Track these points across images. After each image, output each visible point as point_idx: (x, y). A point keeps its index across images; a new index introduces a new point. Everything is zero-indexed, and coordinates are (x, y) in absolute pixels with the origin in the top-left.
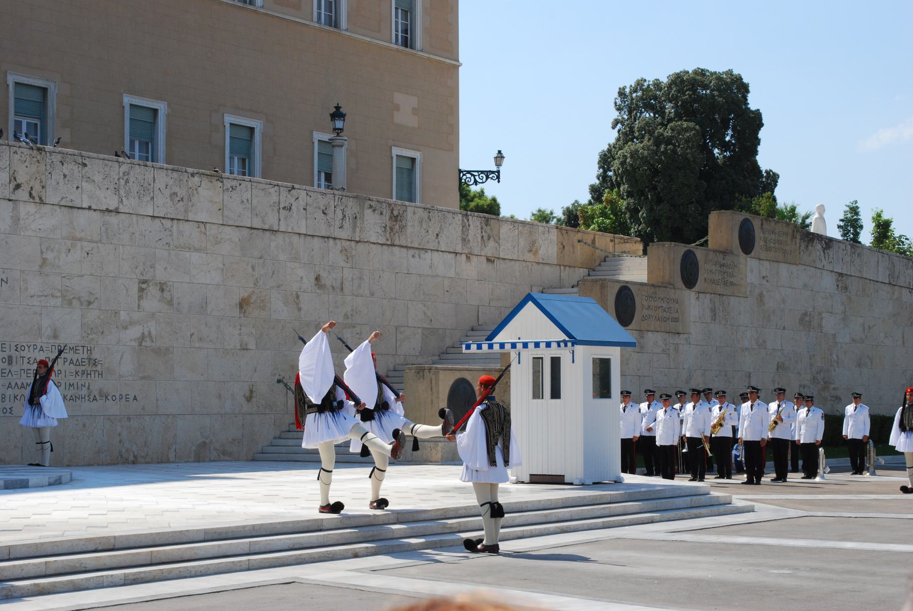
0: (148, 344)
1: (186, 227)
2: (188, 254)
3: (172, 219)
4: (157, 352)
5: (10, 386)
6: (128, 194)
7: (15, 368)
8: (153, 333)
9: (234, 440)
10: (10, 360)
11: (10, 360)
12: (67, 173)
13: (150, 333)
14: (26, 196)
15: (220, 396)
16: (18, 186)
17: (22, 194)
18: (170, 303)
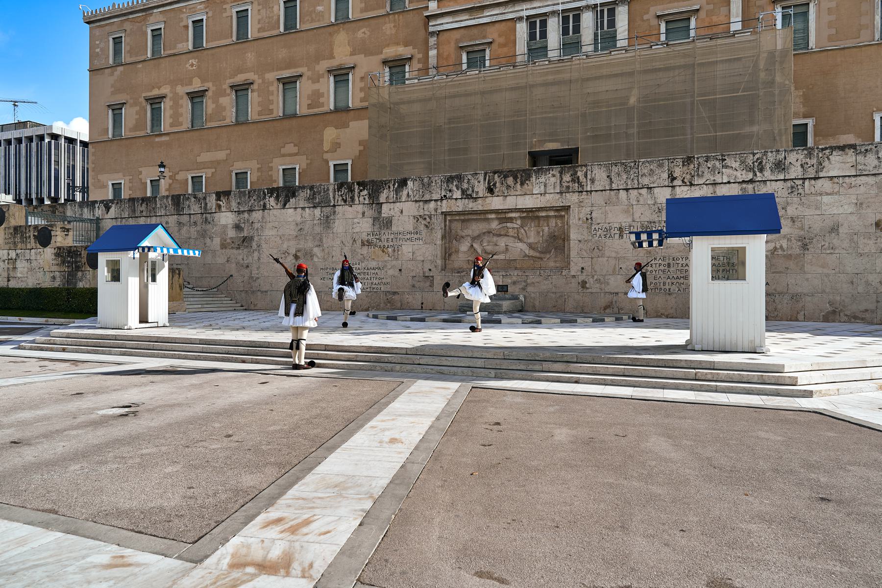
0: (780, 252)
1: (820, 182)
2: (819, 198)
3: (804, 179)
4: (789, 257)
5: (669, 278)
6: (761, 170)
7: (672, 269)
8: (785, 246)
9: (866, 310)
10: (669, 265)
11: (669, 265)
12: (709, 165)
13: (781, 247)
14: (680, 183)
15: (852, 283)
16: (675, 178)
17: (677, 182)
18: (802, 228)
